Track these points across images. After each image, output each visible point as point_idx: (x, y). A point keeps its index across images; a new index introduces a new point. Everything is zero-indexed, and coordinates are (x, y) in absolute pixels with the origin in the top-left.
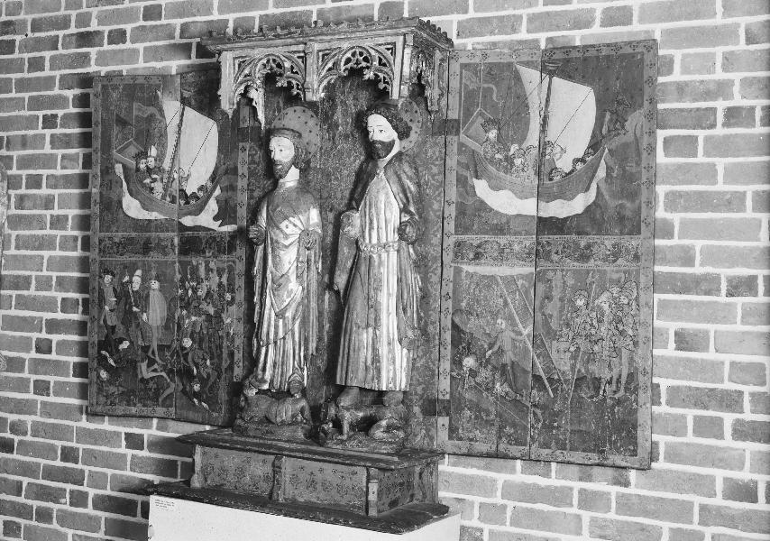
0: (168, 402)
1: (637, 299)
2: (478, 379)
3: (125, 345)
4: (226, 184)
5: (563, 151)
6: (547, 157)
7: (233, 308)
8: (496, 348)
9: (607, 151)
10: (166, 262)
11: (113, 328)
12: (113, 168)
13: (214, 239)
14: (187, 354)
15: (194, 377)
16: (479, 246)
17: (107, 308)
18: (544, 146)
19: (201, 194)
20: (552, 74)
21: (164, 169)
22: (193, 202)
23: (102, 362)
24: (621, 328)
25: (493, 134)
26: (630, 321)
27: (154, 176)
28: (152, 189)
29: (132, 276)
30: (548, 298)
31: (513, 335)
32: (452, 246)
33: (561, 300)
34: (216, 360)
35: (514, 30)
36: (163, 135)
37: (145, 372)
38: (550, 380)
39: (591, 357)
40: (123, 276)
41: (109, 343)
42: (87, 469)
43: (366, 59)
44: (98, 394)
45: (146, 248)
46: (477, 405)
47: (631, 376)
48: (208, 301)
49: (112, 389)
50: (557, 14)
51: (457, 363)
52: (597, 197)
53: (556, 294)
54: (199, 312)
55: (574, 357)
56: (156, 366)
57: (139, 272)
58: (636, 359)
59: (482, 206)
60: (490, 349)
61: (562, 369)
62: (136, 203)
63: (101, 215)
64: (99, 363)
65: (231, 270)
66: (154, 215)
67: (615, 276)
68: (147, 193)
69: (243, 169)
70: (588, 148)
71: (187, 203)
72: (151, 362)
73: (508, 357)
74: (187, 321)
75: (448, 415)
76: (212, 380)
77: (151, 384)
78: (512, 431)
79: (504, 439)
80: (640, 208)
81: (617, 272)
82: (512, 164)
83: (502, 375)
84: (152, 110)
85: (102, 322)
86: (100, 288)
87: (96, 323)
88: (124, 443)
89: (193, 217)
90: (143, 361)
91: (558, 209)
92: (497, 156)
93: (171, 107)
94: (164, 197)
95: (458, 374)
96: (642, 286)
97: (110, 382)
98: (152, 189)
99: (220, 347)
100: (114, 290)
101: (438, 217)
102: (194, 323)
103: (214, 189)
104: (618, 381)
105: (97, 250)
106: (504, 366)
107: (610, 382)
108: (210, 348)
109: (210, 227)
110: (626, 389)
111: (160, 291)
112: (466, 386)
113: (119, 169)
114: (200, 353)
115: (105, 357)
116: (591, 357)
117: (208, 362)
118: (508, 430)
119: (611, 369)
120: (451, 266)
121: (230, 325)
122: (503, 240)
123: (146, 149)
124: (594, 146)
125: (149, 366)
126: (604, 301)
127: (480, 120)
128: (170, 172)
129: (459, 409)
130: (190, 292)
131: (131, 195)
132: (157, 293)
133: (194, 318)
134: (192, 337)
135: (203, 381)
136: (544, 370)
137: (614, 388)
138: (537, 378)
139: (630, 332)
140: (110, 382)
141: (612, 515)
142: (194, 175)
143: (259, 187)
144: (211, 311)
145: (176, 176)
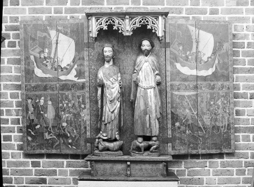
0: (57, 148)
1: (229, 101)
2: (180, 130)
3: (38, 127)
5: (204, 54)
6: (199, 56)
7: (85, 111)
8: (186, 119)
9: (218, 55)
10: (54, 94)
11: (33, 120)
12: (30, 57)
13: (75, 84)
14: (65, 129)
15: (68, 137)
16: (179, 85)
17: (30, 112)
18: (198, 52)
19: (68, 67)
20: (199, 29)
21: (50, 58)
23: (29, 134)
24: (225, 110)
25: (181, 48)
26: (228, 107)
27: (48, 60)
28: (47, 65)
29: (40, 100)
30: (202, 102)
31: (191, 115)
32: (170, 85)
33: (206, 102)
34: (78, 130)
35: (180, 13)
36: (50, 44)
37: (47, 136)
38: (204, 128)
39: (216, 120)
40: (36, 100)
41: (31, 126)
42: (13, 177)
43: (147, 21)
44: (27, 146)
45: (45, 88)
46: (181, 138)
47: (228, 125)
48: (74, 108)
49: (34, 144)
50: (195, 9)
51: (173, 124)
52: (216, 69)
53: (205, 101)
54: (70, 113)
55: (211, 120)
56: (51, 134)
57: (43, 98)
58: (230, 119)
59: (179, 73)
60: (184, 119)
61: (207, 124)
62: (41, 71)
63: (25, 76)
64: (27, 134)
65: (84, 97)
66: (48, 76)
67: (222, 94)
68: (44, 67)
69: (86, 58)
70: (212, 54)
71: (62, 71)
72: (50, 133)
73: (190, 122)
74: (64, 116)
75: (171, 142)
76: (77, 138)
77: (50, 141)
78: (193, 145)
79: (190, 148)
80: (229, 73)
81: (223, 93)
82: (188, 58)
83: (189, 128)
84: (45, 34)
85: (28, 118)
86: (26, 105)
87: (25, 118)
88: (31, 165)
89: (65, 76)
90: (46, 132)
91: (204, 73)
92: (183, 55)
93: (53, 33)
94: (52, 68)
95: (174, 129)
96: (230, 97)
97: (32, 141)
98: (47, 65)
99: (80, 125)
100: (33, 105)
101: (164, 76)
102: (68, 117)
104: (225, 127)
105: (24, 90)
106: (189, 125)
107: (222, 127)
108: (75, 126)
109: (73, 80)
110: (227, 129)
111: (52, 105)
112: (177, 132)
114: (71, 128)
115: (30, 132)
116: (216, 120)
117: (75, 131)
118: (191, 145)
119: (222, 123)
120: (170, 93)
121: (84, 117)
122: (186, 83)
123: (43, 49)
124: (214, 53)
125: (49, 134)
126: (219, 102)
127: (177, 43)
128: (54, 59)
129: (175, 140)
130: (65, 105)
131: (38, 68)
132: (51, 106)
133: (67, 115)
134: (67, 122)
135: (73, 139)
136: (202, 125)
137: (224, 129)
138: (200, 128)
139: (228, 111)
140: (32, 141)
141: (219, 168)
143: (94, 65)
144: (75, 112)
145: (56, 60)
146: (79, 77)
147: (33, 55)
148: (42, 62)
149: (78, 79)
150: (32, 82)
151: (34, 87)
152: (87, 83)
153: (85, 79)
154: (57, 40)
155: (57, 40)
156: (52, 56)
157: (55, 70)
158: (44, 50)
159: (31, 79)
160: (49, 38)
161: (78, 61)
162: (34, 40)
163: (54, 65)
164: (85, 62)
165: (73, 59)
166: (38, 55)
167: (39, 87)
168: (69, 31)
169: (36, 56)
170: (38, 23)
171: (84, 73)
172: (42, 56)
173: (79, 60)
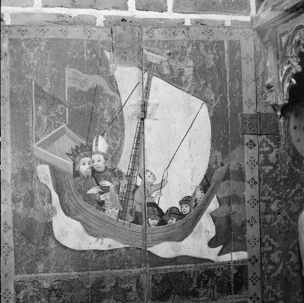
4: (226, 195)
12: (33, 172)
13: (210, 273)
19: (186, 209)
21: (120, 172)
27: (107, 183)
36: (118, 119)
62: (77, 225)
66: (106, 244)
68: (92, 210)
69: (251, 174)
71: (162, 223)
89: (174, 243)
94: (121, 215)
98: (102, 203)
113: (43, 172)
123: (89, 140)
128: (130, 177)
131: (68, 213)
142: (174, 181)
143: (279, 198)
145: (139, 182)
146: (225, 245)
147: (48, 164)
148: (82, 192)
149: (221, 253)
150: (46, 271)
151: (51, 290)
152: (253, 264)
153: (245, 250)
154: (144, 105)
155: (144, 105)
156: (124, 165)
157: (137, 221)
158: (92, 141)
159: (37, 258)
160: (112, 94)
161: (223, 185)
162: (53, 101)
163: (130, 202)
164: (247, 186)
165: (202, 176)
166: (66, 164)
167: (71, 289)
168: (189, 72)
169: (53, 164)
170: (70, 36)
171: (242, 229)
172: (84, 169)
173: (224, 181)
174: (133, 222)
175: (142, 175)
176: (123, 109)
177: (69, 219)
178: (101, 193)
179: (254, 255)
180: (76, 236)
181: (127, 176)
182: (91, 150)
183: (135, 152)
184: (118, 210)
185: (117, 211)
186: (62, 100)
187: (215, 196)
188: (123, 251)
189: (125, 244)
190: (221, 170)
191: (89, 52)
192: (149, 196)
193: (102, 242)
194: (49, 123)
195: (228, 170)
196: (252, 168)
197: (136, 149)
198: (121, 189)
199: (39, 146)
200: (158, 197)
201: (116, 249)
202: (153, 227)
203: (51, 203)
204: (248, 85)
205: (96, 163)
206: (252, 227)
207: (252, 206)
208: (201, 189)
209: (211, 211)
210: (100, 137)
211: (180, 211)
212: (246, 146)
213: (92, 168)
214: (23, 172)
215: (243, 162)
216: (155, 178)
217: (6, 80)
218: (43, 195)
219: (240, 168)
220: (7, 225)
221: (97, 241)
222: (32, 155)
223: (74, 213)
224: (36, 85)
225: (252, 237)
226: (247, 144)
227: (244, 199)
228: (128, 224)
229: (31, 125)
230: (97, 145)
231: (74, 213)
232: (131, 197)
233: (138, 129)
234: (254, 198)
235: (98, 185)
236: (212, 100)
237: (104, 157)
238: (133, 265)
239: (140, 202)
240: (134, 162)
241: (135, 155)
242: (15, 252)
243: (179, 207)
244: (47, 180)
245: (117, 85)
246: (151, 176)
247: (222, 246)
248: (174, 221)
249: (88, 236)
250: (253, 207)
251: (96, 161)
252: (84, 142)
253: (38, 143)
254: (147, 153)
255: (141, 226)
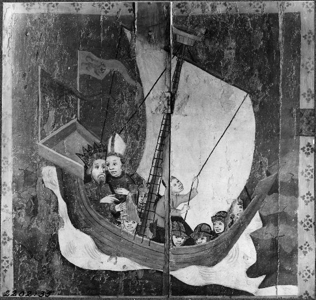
12: (39, 175)
19: (220, 227)
21: (140, 179)
22: (202, 241)
27: (123, 191)
62: (87, 240)
66: (121, 264)
68: (105, 223)
71: (190, 242)
89: (203, 268)
94: (140, 230)
98: (117, 215)
103: (247, 218)
109: (241, 288)
113: (50, 177)
123: (104, 137)
128: (153, 184)
131: (76, 224)
145: (162, 191)
146: (268, 275)
147: (56, 166)
148: (95, 201)
149: (262, 286)
156: (145, 170)
160: (133, 83)
161: (269, 200)
163: (151, 215)
164: (301, 202)
165: (243, 188)
168: (230, 54)
169: (62, 165)
171: (292, 256)
172: (97, 173)
173: (270, 193)
174: (153, 240)
175: (167, 185)
176: (146, 101)
177: (78, 231)
178: (116, 203)
179: (306, 292)
180: (85, 253)
181: (148, 183)
182: (106, 150)
183: (159, 155)
184: (136, 224)
185: (135, 226)
186: (73, 89)
187: (258, 213)
188: (141, 275)
189: (144, 265)
190: (266, 180)
191: (106, 30)
192: (175, 209)
193: (116, 262)
194: (57, 118)
195: (276, 181)
196: (308, 180)
197: (160, 150)
198: (140, 199)
199: (44, 144)
200: (185, 209)
201: (133, 271)
202: (178, 246)
203: (58, 213)
204: (308, 72)
205: (111, 167)
206: (305, 255)
207: (306, 228)
208: (240, 203)
209: (252, 231)
210: (117, 135)
211: (212, 230)
212: (301, 151)
213: (107, 172)
214: (26, 174)
215: (297, 172)
216: (182, 187)
217: (8, 64)
218: (49, 202)
219: (293, 180)
220: (6, 235)
221: (110, 259)
222: (37, 154)
223: (84, 224)
224: (42, 70)
225: (305, 269)
226: (303, 149)
227: (296, 218)
228: (146, 241)
229: (36, 119)
230: (113, 145)
231: (84, 224)
232: (152, 209)
233: (163, 126)
234: (310, 218)
235: (113, 193)
236: (258, 91)
237: (121, 160)
238: (153, 292)
239: (163, 216)
240: (157, 167)
241: (158, 159)
242: (14, 266)
243: (211, 224)
244: (54, 185)
245: (139, 73)
246: (178, 184)
247: (264, 276)
248: (204, 241)
249: (99, 253)
250: (307, 230)
251: (111, 164)
252: (98, 141)
253: (43, 141)
254: (173, 156)
255: (163, 244)
